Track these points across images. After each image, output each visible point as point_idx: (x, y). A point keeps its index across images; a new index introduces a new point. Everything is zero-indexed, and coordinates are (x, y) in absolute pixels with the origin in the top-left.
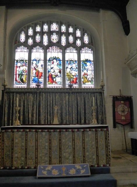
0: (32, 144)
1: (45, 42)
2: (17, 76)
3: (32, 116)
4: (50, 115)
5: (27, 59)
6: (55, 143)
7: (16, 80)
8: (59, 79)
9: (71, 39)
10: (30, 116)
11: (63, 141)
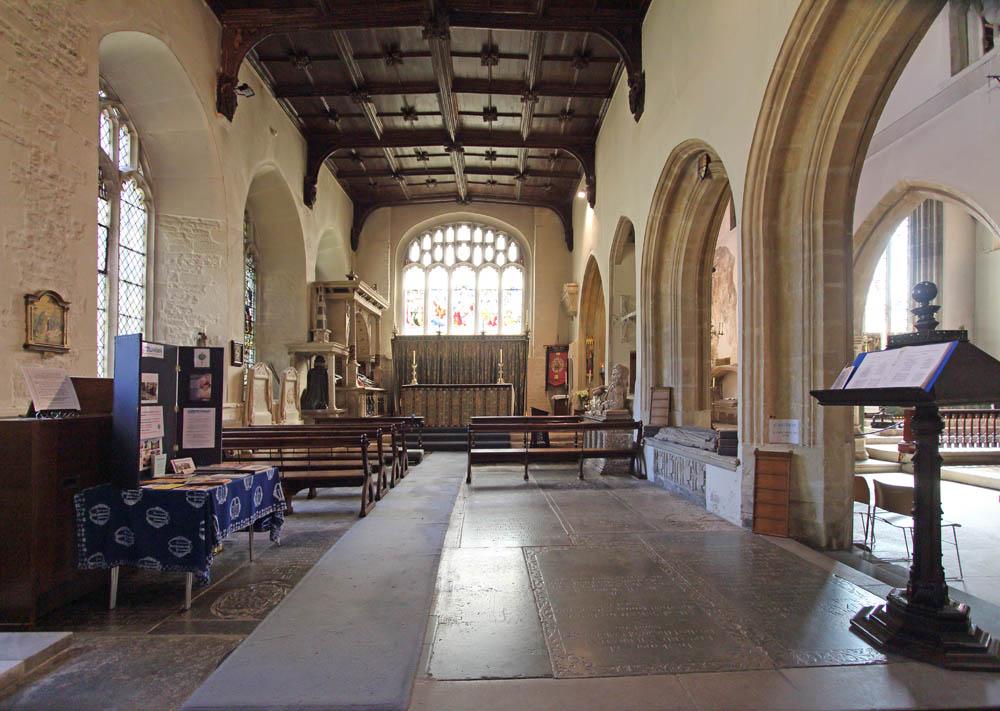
0: (432, 402)
1: (450, 261)
2: (409, 314)
3: (432, 373)
4: (455, 373)
5: (423, 289)
6: (456, 402)
7: (408, 322)
8: (469, 319)
9: (489, 253)
10: (429, 373)
11: (464, 400)
